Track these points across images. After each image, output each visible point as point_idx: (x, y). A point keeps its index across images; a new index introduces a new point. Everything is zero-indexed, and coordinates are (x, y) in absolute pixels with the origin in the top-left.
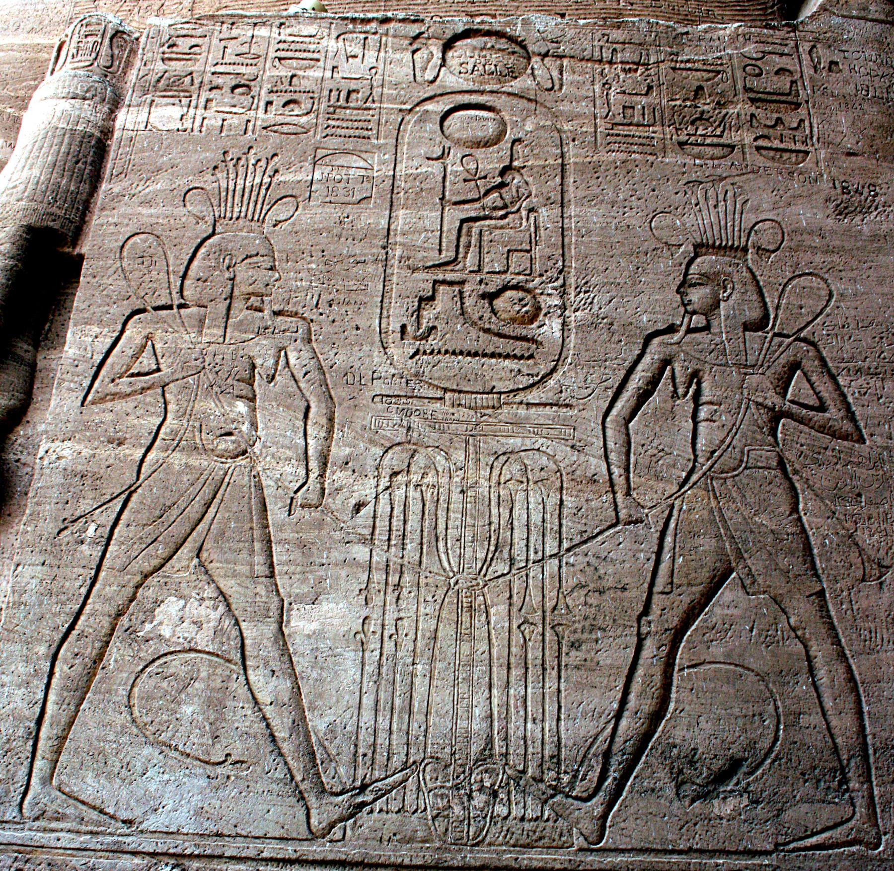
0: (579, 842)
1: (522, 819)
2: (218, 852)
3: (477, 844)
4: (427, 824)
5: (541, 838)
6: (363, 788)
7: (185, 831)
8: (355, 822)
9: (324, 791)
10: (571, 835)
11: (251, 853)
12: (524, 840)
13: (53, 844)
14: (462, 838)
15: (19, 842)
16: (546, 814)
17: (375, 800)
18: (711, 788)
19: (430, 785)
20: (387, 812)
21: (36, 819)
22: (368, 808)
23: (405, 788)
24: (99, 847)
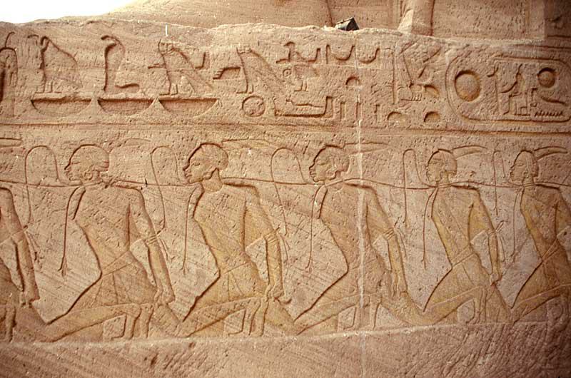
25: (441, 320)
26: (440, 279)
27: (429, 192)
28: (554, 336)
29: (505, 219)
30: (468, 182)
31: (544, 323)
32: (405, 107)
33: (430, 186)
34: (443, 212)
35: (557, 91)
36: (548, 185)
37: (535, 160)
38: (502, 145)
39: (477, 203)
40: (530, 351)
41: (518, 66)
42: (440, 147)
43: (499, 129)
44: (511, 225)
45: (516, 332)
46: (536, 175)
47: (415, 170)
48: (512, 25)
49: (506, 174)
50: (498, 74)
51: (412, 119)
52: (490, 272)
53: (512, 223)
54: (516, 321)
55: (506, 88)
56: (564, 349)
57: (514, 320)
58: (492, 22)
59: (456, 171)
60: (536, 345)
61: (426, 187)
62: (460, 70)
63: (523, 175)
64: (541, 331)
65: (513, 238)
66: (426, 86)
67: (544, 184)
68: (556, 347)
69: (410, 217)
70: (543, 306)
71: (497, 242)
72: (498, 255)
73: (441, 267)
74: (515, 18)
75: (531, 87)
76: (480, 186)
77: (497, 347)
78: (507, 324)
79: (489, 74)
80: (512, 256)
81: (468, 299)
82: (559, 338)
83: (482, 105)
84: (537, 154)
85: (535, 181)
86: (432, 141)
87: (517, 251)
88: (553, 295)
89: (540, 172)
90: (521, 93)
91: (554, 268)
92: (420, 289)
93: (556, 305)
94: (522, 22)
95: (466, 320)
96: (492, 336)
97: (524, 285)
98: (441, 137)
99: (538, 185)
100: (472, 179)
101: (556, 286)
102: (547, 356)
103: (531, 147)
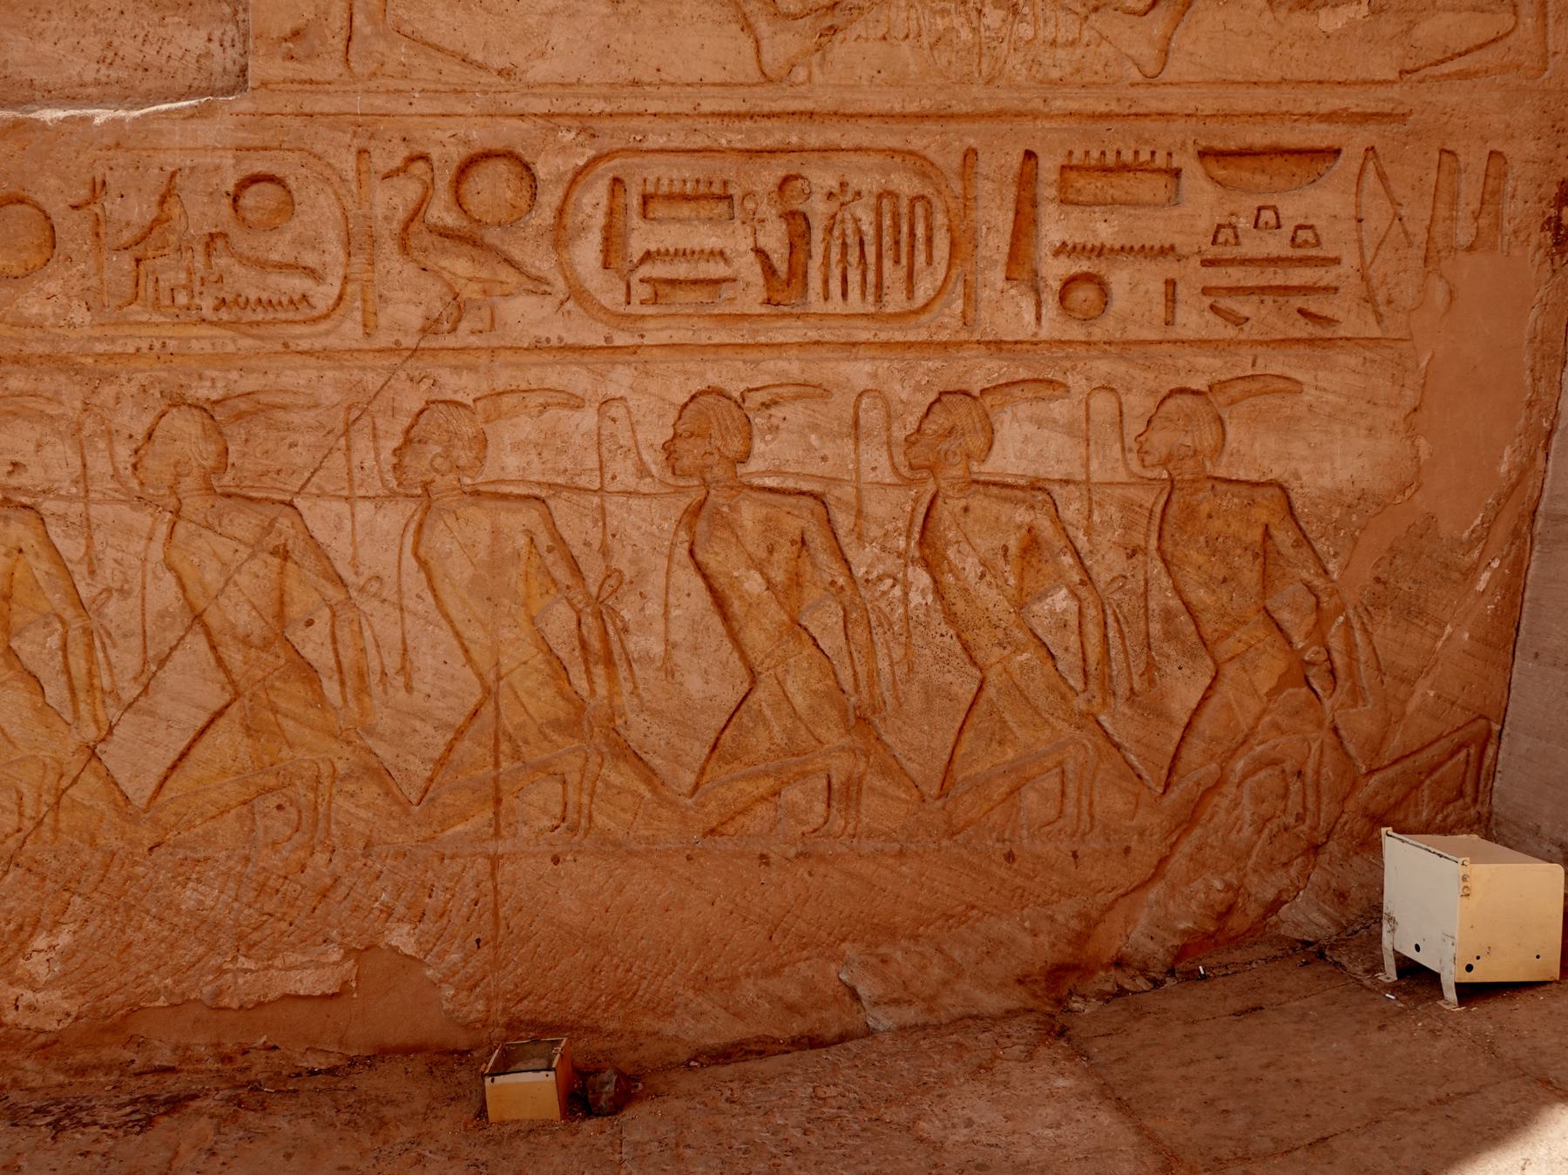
1: (1053, 43)
7: (588, 81)
11: (686, 107)
20: (867, 39)
29: (117, 585)
36: (253, 494)
44: (134, 602)
48: (208, 54)
49: (121, 466)
55: (126, 237)
58: (150, 51)
65: (139, 630)
67: (244, 492)
74: (217, 35)
80: (135, 679)
97: (183, 755)
100: (13, 482)
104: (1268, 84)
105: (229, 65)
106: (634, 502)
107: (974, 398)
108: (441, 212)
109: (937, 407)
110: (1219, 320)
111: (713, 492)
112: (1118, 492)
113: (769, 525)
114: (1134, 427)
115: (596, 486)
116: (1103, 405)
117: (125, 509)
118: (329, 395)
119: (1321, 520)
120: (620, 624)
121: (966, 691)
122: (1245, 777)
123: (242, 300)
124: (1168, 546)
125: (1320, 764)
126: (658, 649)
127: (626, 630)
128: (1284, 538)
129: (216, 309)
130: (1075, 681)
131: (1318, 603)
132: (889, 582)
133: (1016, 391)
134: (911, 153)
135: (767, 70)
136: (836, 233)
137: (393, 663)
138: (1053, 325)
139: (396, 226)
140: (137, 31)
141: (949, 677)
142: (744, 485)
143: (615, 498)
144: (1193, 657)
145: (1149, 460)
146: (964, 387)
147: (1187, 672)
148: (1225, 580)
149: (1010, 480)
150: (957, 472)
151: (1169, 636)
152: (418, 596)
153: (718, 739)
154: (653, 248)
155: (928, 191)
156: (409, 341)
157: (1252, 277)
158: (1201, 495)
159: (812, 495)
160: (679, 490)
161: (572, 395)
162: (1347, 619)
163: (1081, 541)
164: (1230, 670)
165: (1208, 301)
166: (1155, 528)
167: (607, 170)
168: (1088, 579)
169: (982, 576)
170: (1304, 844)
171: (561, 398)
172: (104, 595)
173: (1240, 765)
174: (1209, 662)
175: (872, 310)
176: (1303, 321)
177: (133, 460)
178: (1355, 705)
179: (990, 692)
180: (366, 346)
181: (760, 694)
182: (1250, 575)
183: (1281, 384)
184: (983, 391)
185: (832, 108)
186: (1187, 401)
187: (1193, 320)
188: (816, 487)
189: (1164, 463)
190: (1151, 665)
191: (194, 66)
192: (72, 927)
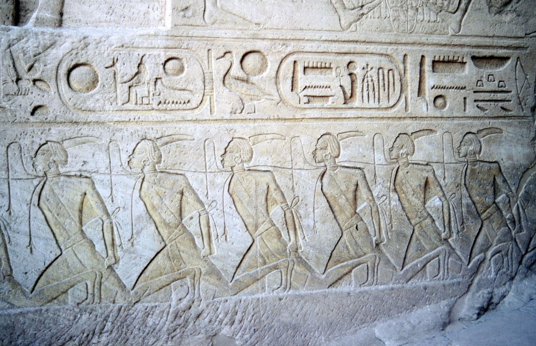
0: (451, 32)
2: (302, 38)
3: (411, 33)
4: (390, 24)
5: (436, 30)
6: (362, 6)
8: (360, 23)
9: (345, 8)
10: (448, 29)
12: (430, 31)
13: (224, 35)
14: (405, 30)
15: (207, 36)
16: (438, 19)
17: (368, 12)
18: (502, 9)
19: (391, 5)
21: (213, 23)
22: (365, 16)
23: (380, 7)
24: (247, 37)
25: (49, 301)
26: (48, 263)
27: (36, 182)
28: (176, 316)
30: (80, 171)
31: (167, 304)
32: (11, 102)
33: (37, 177)
34: (51, 200)
35: (184, 79)
36: (171, 171)
37: (156, 149)
38: (118, 135)
39: (90, 191)
40: (152, 330)
41: (141, 56)
42: (48, 139)
43: (116, 119)
44: (128, 212)
45: (135, 313)
46: (159, 162)
47: (20, 162)
48: (148, 13)
50: (118, 65)
51: (18, 114)
52: (104, 255)
53: (130, 209)
54: (137, 302)
55: (126, 78)
56: (189, 327)
57: (133, 301)
58: (126, 10)
59: (66, 161)
60: (158, 324)
61: (33, 177)
62: (74, 63)
63: (142, 163)
64: (163, 312)
65: (130, 223)
66: (35, 81)
67: (168, 171)
68: (179, 325)
69: (14, 206)
70: (168, 287)
71: (112, 228)
72: (113, 240)
73: (49, 252)
75: (155, 77)
76: (93, 175)
77: (114, 327)
78: (125, 305)
79: (106, 66)
81: (79, 282)
82: (182, 318)
83: (97, 97)
84: (159, 143)
85: (157, 168)
86: (39, 133)
87: (135, 236)
88: (178, 277)
89: (163, 159)
90: (144, 83)
91: (179, 251)
92: (26, 273)
93: (182, 286)
94: (159, 10)
95: (78, 301)
96: (108, 316)
98: (50, 129)
99: (162, 172)
100: (84, 168)
101: (182, 269)
102: (169, 335)
103: (152, 135)
104: (490, 37)
105: (156, 17)
106: (303, 172)
107: (409, 136)
108: (236, 71)
109: (398, 138)
110: (479, 110)
111: (328, 168)
112: (452, 165)
113: (348, 179)
114: (456, 145)
115: (290, 167)
116: (446, 136)
117: (125, 177)
118: (198, 135)
119: (509, 173)
120: (299, 216)
121: (409, 233)
122: (492, 256)
123: (167, 102)
124: (467, 182)
125: (512, 252)
126: (312, 223)
127: (301, 217)
128: (499, 181)
129: (158, 105)
130: (441, 229)
131: (509, 200)
132: (385, 197)
133: (421, 133)
134: (387, 55)
135: (343, 27)
136: (366, 80)
137: (220, 231)
138: (432, 111)
139: (222, 76)
140: (121, 3)
141: (404, 229)
142: (338, 166)
143: (297, 171)
144: (476, 218)
145: (461, 155)
146: (406, 132)
147: (474, 223)
148: (484, 194)
149: (421, 163)
150: (405, 160)
151: (469, 212)
152: (230, 207)
153: (331, 254)
154: (308, 85)
155: (394, 68)
156: (228, 116)
157: (487, 96)
158: (476, 167)
159: (359, 168)
160: (318, 168)
161: (282, 135)
162: (518, 206)
163: (442, 182)
164: (486, 223)
165: (476, 103)
166: (463, 177)
167: (291, 59)
168: (444, 195)
169: (413, 195)
170: (509, 277)
171: (278, 136)
172: (117, 210)
173: (489, 254)
174: (480, 220)
175: (378, 106)
176: (502, 111)
177: (128, 160)
178: (521, 232)
179: (416, 232)
180: (211, 118)
181: (345, 237)
182: (491, 192)
183: (498, 131)
184: (412, 133)
185: (363, 40)
186: (470, 136)
187: (471, 110)
188: (361, 166)
189: (465, 156)
190: (463, 223)
191: (142, 17)
192: (107, 334)
